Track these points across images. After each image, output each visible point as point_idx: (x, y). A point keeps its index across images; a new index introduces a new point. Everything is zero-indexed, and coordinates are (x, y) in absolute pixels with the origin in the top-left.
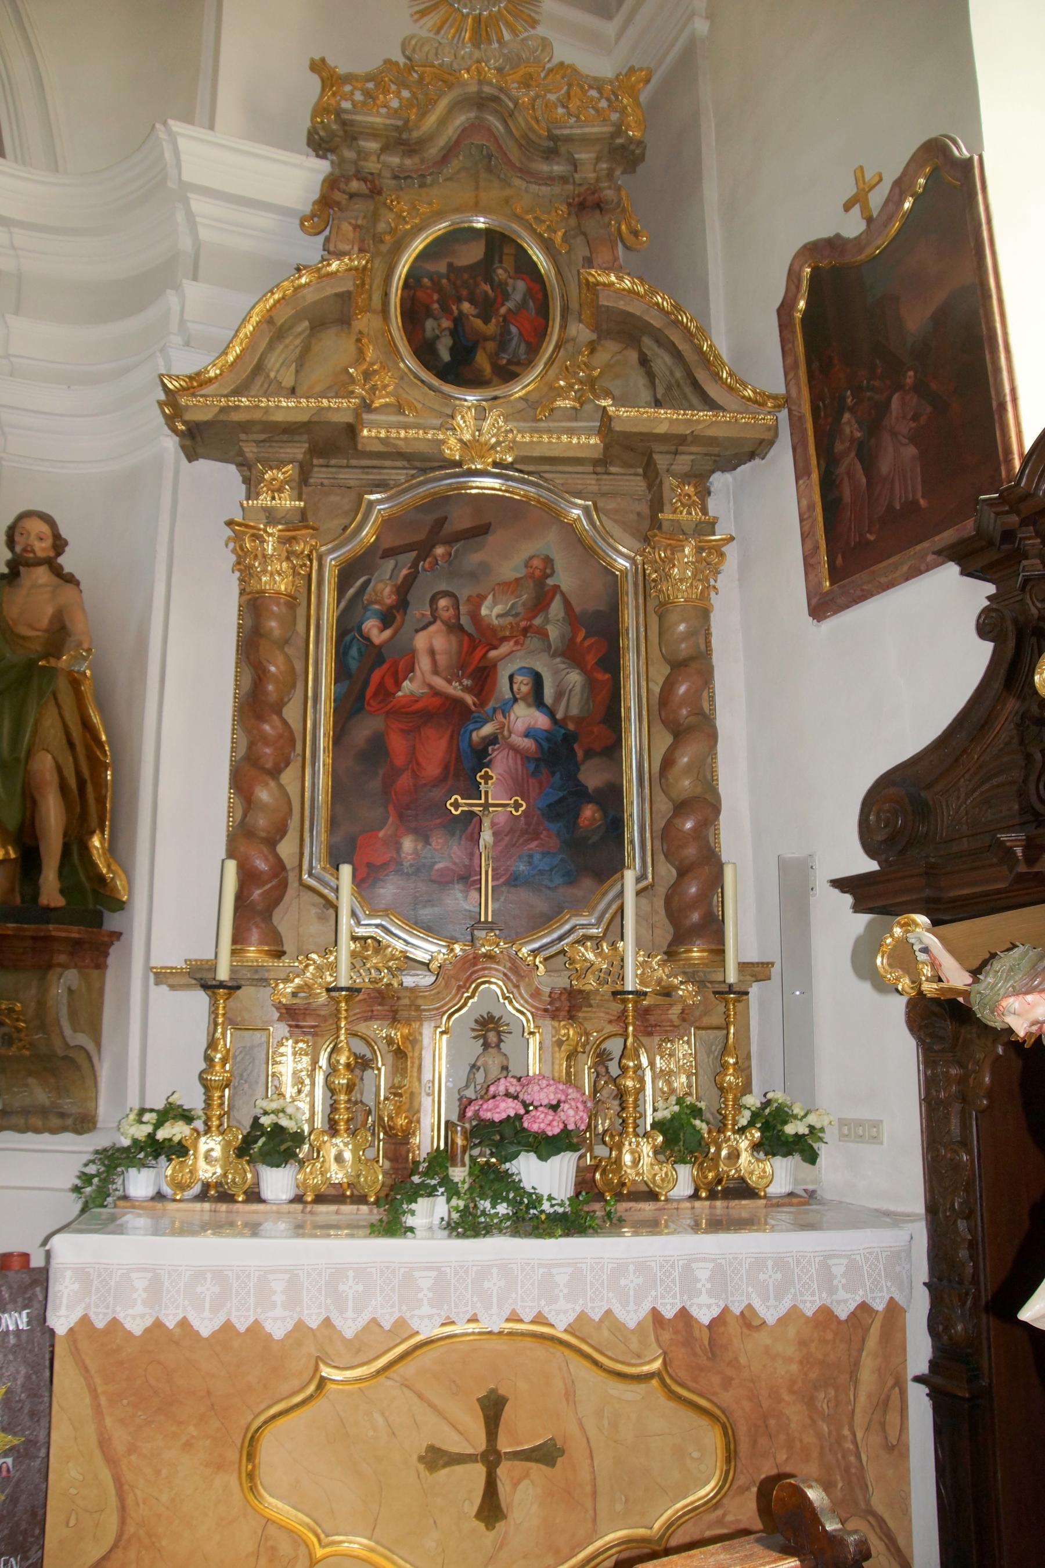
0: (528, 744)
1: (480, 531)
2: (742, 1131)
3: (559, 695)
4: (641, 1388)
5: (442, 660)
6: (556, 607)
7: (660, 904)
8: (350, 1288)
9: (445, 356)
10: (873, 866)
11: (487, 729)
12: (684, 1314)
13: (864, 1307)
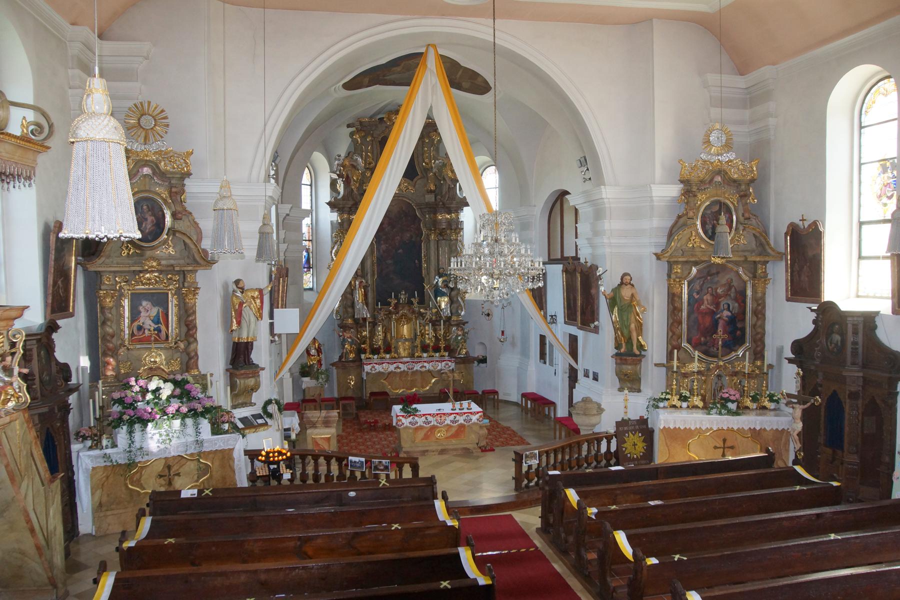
0: (727, 319)
1: (718, 273)
2: (765, 398)
3: (733, 308)
4: (746, 439)
5: (709, 301)
6: (733, 290)
7: (752, 351)
8: (704, 423)
9: (710, 232)
10: (794, 356)
11: (718, 316)
12: (754, 428)
13: (783, 429)
